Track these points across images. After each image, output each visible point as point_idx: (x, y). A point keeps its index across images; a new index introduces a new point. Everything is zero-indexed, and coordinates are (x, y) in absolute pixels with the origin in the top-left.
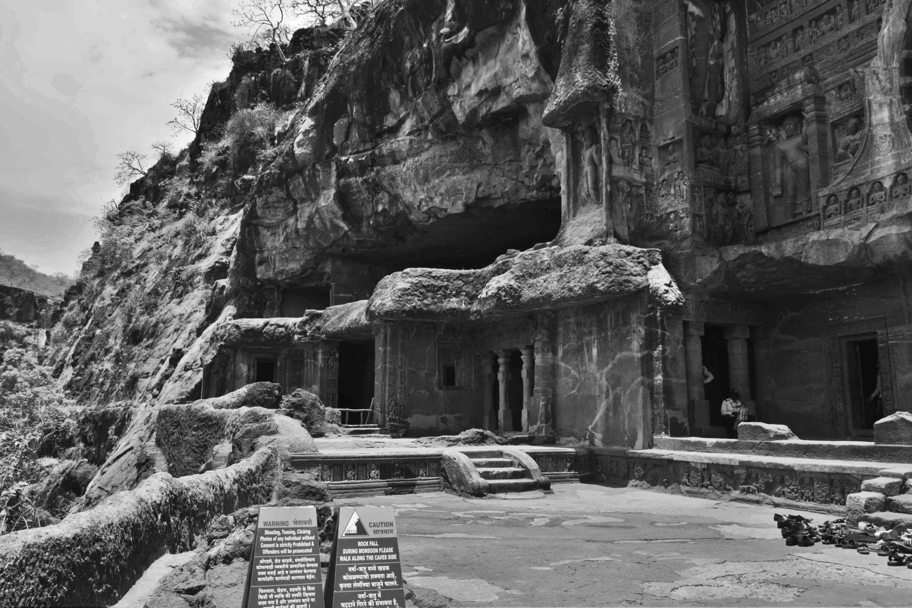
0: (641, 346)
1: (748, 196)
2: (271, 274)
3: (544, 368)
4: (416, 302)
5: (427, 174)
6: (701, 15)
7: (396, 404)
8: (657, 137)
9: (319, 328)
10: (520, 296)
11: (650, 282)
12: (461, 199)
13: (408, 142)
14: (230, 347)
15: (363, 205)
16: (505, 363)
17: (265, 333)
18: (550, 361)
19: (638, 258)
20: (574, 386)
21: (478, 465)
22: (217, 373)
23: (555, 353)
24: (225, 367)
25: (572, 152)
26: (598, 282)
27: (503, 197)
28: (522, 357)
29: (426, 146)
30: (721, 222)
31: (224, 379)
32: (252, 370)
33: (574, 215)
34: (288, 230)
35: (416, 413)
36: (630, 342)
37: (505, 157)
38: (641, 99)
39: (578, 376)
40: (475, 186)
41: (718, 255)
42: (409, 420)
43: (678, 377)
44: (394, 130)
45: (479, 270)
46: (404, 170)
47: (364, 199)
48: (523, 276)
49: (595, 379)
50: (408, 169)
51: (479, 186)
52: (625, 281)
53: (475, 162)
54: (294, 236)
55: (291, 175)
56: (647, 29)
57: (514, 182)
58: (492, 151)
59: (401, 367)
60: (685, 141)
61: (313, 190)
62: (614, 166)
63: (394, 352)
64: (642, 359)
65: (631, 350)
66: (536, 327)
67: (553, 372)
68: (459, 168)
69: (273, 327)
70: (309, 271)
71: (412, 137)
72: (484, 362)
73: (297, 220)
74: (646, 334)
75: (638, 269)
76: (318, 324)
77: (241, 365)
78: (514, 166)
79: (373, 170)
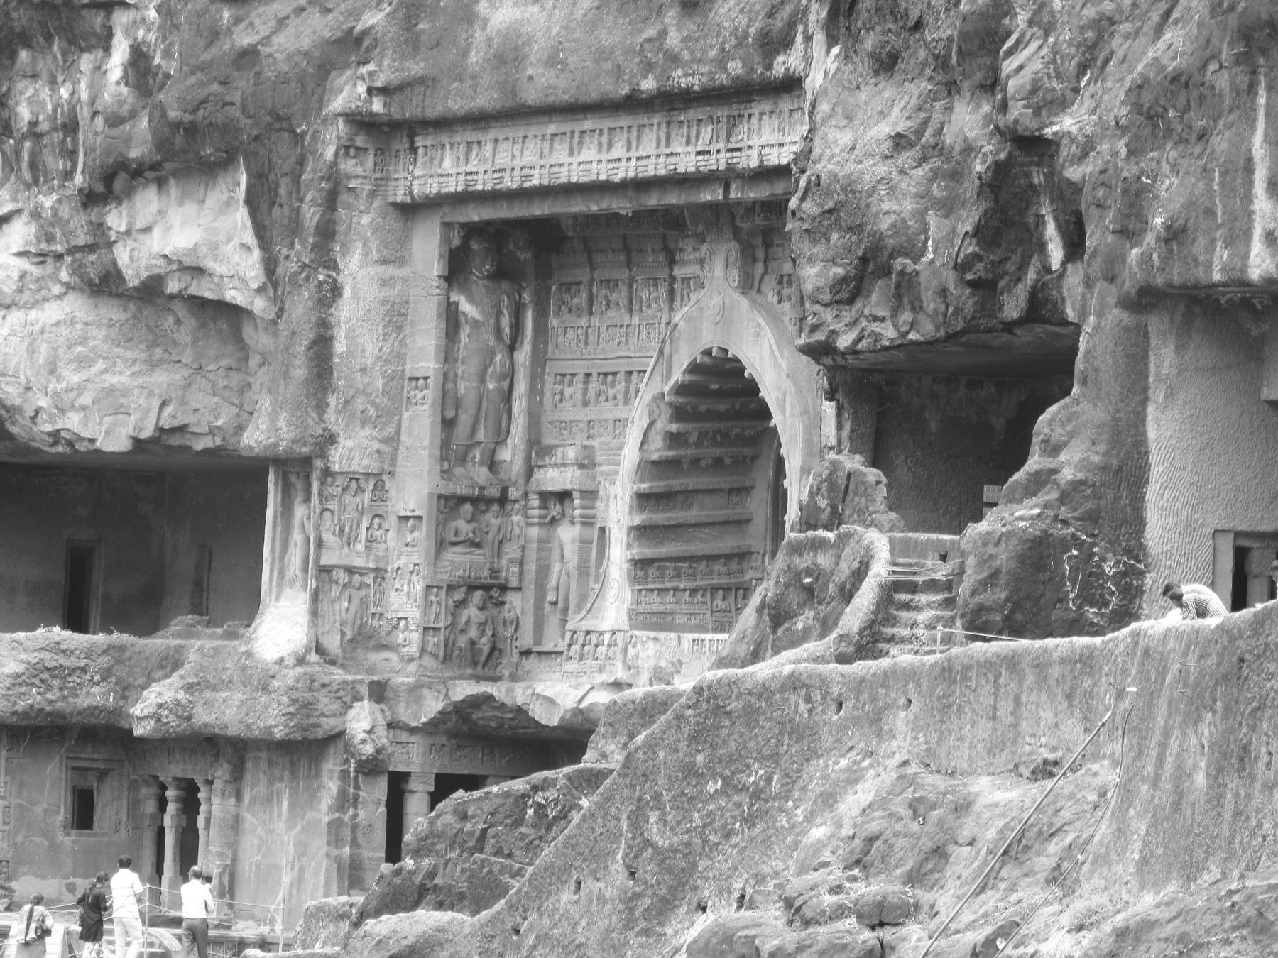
0: (330, 808)
1: (519, 595)
3: (224, 820)
4: (34, 698)
5: (55, 357)
6: (478, 317)
10: (189, 718)
13: (16, 275)
18: (232, 810)
19: (337, 691)
20: (259, 850)
23: (239, 796)
25: (283, 500)
26: (276, 726)
28: (200, 795)
29: (57, 289)
33: (277, 599)
35: (25, 874)
36: (320, 802)
37: (218, 358)
38: (376, 446)
40: (156, 403)
41: (444, 691)
42: (14, 885)
43: (373, 850)
45: (142, 641)
48: (199, 683)
51: (164, 404)
52: (312, 725)
53: (158, 353)
56: (399, 329)
57: (235, 410)
58: (195, 341)
60: (425, 520)
62: (324, 551)
64: (330, 824)
66: (217, 755)
67: (235, 825)
68: (125, 360)
71: (24, 264)
74: (339, 791)
75: (336, 706)
78: (236, 379)
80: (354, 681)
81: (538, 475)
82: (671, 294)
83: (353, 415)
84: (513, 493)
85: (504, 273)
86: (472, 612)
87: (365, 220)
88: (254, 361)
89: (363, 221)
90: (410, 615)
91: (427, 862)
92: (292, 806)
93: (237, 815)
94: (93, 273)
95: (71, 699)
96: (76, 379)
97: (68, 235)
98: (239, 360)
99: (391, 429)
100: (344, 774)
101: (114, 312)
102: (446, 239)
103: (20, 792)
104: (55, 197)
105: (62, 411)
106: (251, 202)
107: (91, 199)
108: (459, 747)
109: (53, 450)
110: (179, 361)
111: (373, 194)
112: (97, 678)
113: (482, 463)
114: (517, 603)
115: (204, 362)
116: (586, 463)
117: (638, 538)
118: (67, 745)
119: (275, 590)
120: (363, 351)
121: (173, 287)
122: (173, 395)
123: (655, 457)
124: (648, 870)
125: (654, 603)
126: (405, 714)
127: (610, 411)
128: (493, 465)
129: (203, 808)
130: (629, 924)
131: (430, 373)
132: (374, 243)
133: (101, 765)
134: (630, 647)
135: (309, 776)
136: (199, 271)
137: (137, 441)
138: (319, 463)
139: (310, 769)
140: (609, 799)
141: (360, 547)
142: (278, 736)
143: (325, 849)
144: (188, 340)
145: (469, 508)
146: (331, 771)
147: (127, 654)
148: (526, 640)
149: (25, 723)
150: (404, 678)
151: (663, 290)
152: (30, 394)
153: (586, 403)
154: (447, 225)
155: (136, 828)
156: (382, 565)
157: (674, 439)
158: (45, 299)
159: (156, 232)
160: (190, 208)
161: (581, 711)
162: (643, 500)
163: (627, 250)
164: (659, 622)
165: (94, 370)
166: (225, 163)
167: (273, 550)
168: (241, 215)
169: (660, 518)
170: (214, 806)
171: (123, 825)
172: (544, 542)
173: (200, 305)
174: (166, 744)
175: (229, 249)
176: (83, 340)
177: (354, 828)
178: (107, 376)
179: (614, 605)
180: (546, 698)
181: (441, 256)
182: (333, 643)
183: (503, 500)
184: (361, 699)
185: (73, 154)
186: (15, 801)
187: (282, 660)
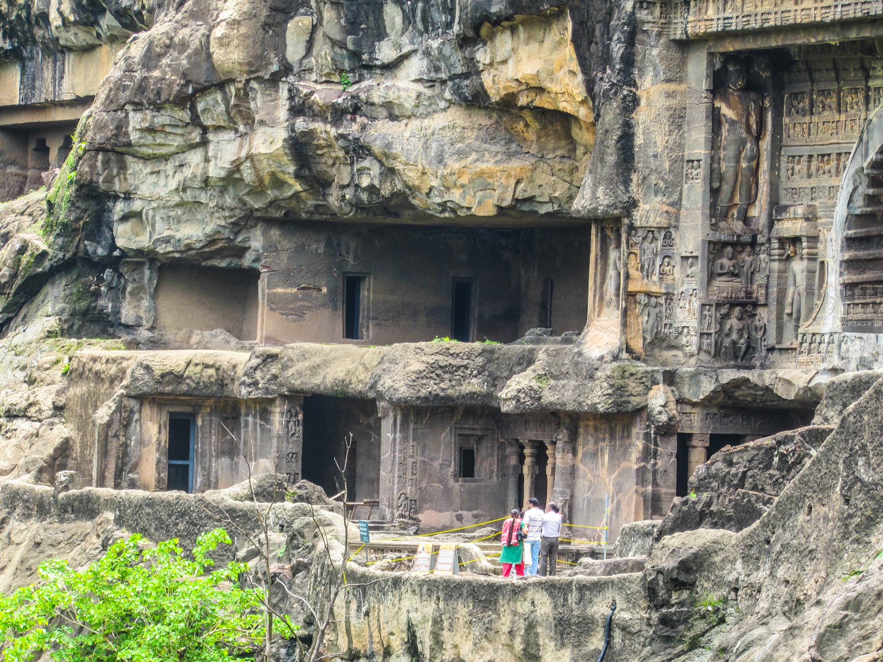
0: (638, 459)
1: (766, 309)
2: (143, 241)
3: (564, 468)
4: (432, 387)
5: (443, 151)
6: (734, 118)
7: (406, 498)
8: (681, 245)
9: (275, 377)
10: (540, 398)
11: (649, 401)
12: (491, 197)
13: (414, 95)
14: (134, 397)
15: (334, 164)
16: (532, 455)
17: (188, 377)
18: (570, 462)
19: (641, 379)
20: (589, 488)
21: (486, 555)
22: (116, 436)
23: (574, 452)
24: (126, 427)
25: (601, 247)
27: (551, 201)
28: (547, 452)
29: (442, 105)
30: (734, 336)
31: (126, 445)
32: (163, 432)
33: (599, 315)
34: (187, 172)
35: (428, 509)
37: (554, 150)
38: (665, 208)
39: (592, 479)
40: (513, 182)
41: (715, 377)
42: (420, 516)
43: (668, 487)
44: (391, 67)
45: (506, 347)
46: (407, 135)
47: (337, 158)
48: (546, 375)
49: (605, 484)
50: (413, 135)
51: (518, 182)
52: (624, 402)
53: (513, 147)
54: (197, 184)
55: (203, 90)
56: (680, 127)
57: (567, 185)
58: (539, 138)
59: (412, 457)
61: (241, 118)
62: (630, 281)
63: (405, 439)
64: (638, 470)
65: (630, 461)
66: (559, 424)
67: (573, 472)
68: (490, 152)
69: (199, 368)
70: (220, 245)
71: (420, 87)
72: (509, 450)
73: (207, 160)
75: (640, 389)
76: (274, 371)
77: (149, 424)
79: (354, 120)
80: (653, 371)
81: (777, 226)
82: (867, 100)
83: (649, 187)
84: (761, 239)
85: (752, 87)
86: (733, 322)
87: (655, 52)
88: (580, 151)
89: (653, 52)
90: (690, 325)
91: (705, 496)
92: (611, 458)
93: (574, 465)
94: (467, 93)
95: (457, 388)
96: (456, 166)
97: (449, 67)
98: (569, 150)
99: (675, 197)
100: (647, 436)
101: (482, 119)
102: (710, 64)
103: (423, 452)
104: (440, 40)
105: (448, 189)
106: (576, 40)
107: (465, 42)
108: (726, 416)
109: (442, 216)
110: (528, 153)
111: (659, 34)
112: (475, 372)
113: (738, 219)
114: (765, 316)
115: (545, 152)
116: (811, 217)
117: (847, 268)
118: (455, 418)
119: (597, 309)
120: (655, 143)
121: (523, 101)
122: (524, 176)
123: (858, 212)
124: (859, 498)
125: (859, 313)
126: (688, 392)
127: (826, 181)
128: (746, 220)
129: (550, 461)
130: (845, 536)
131: (702, 157)
132: (661, 67)
133: (479, 433)
134: (843, 344)
135: (623, 437)
136: (541, 90)
137: (500, 208)
138: (626, 221)
139: (623, 432)
140: (830, 449)
141: (655, 278)
142: (601, 410)
143: (635, 487)
144: (534, 137)
145: (730, 250)
146: (638, 433)
147: (496, 356)
148: (771, 340)
149: (425, 405)
150: (687, 368)
151: (861, 96)
152: (425, 177)
153: (809, 176)
154: (711, 55)
155: (504, 475)
156: (670, 290)
157: (870, 200)
158: (435, 112)
159: (511, 63)
160: (534, 46)
161: (810, 389)
162: (850, 242)
163: (836, 69)
164: (863, 326)
165: (469, 160)
166: (559, 15)
167: (595, 281)
168: (569, 50)
169: (861, 254)
170: (558, 459)
171: (495, 474)
172: (782, 273)
173: (542, 114)
174: (523, 417)
175: (561, 74)
176: (462, 139)
177: (655, 472)
178: (478, 164)
179: (831, 314)
180: (785, 380)
181: (708, 76)
182: (638, 345)
183: (753, 243)
184: (658, 384)
185: (451, 11)
186: (420, 458)
187: (602, 357)
